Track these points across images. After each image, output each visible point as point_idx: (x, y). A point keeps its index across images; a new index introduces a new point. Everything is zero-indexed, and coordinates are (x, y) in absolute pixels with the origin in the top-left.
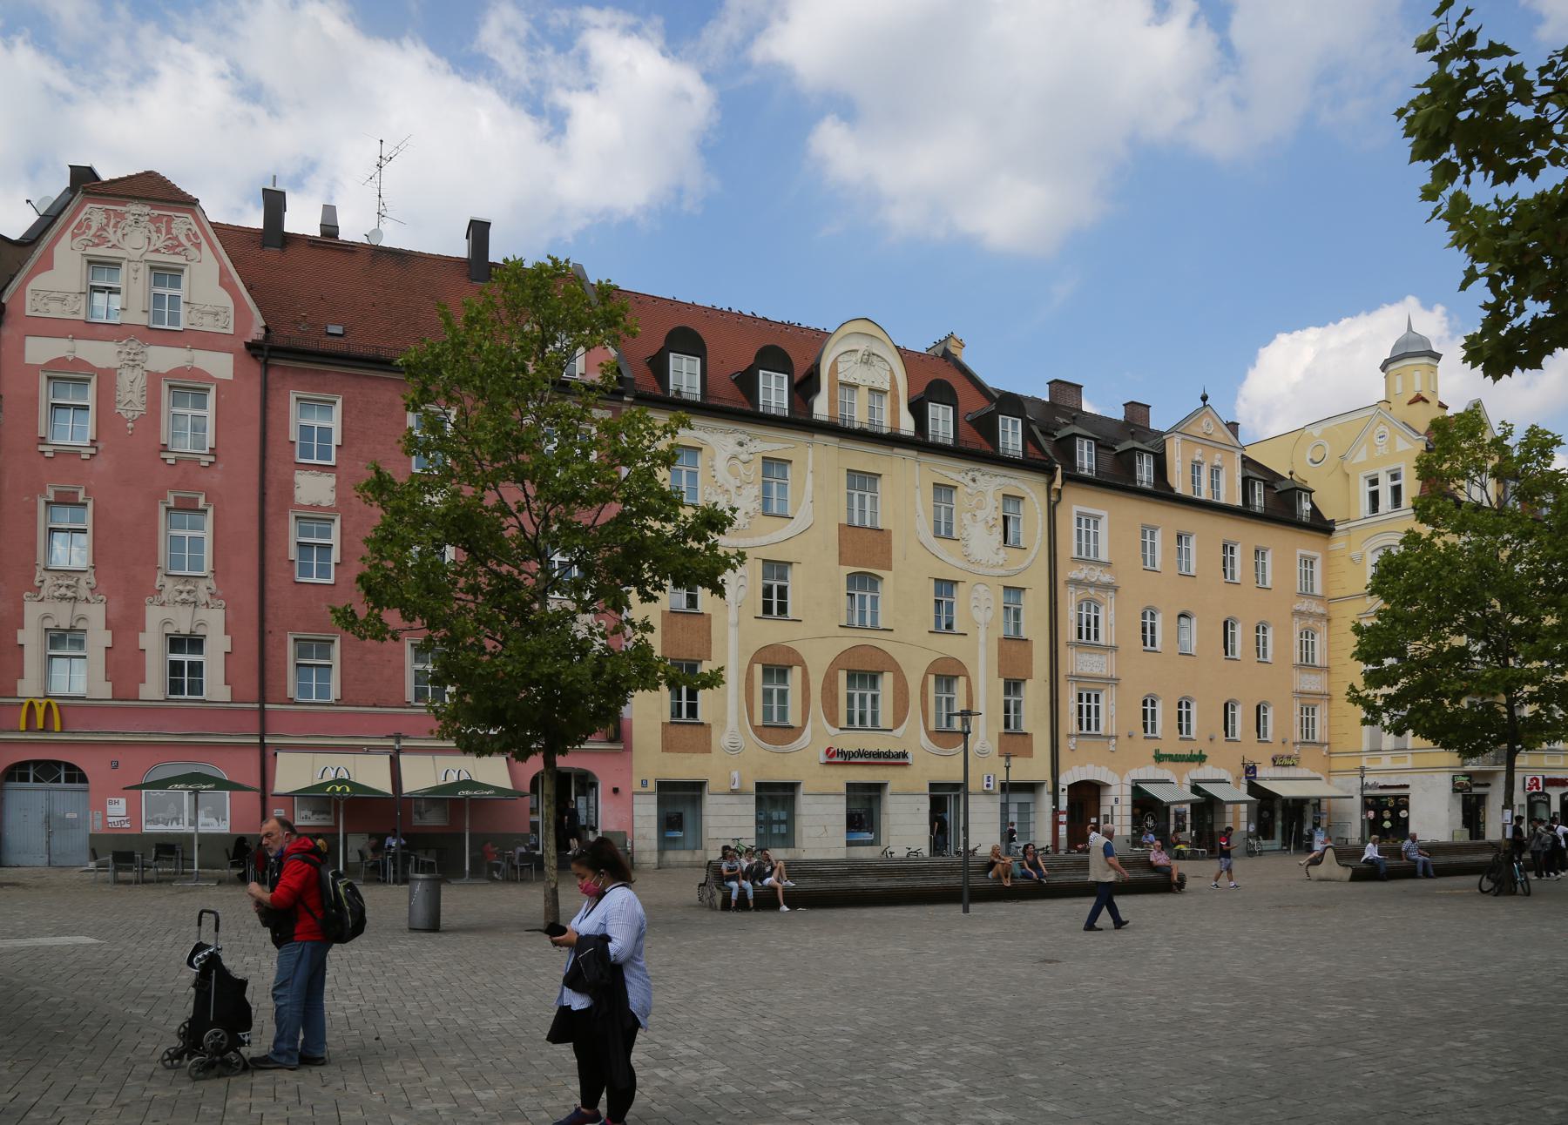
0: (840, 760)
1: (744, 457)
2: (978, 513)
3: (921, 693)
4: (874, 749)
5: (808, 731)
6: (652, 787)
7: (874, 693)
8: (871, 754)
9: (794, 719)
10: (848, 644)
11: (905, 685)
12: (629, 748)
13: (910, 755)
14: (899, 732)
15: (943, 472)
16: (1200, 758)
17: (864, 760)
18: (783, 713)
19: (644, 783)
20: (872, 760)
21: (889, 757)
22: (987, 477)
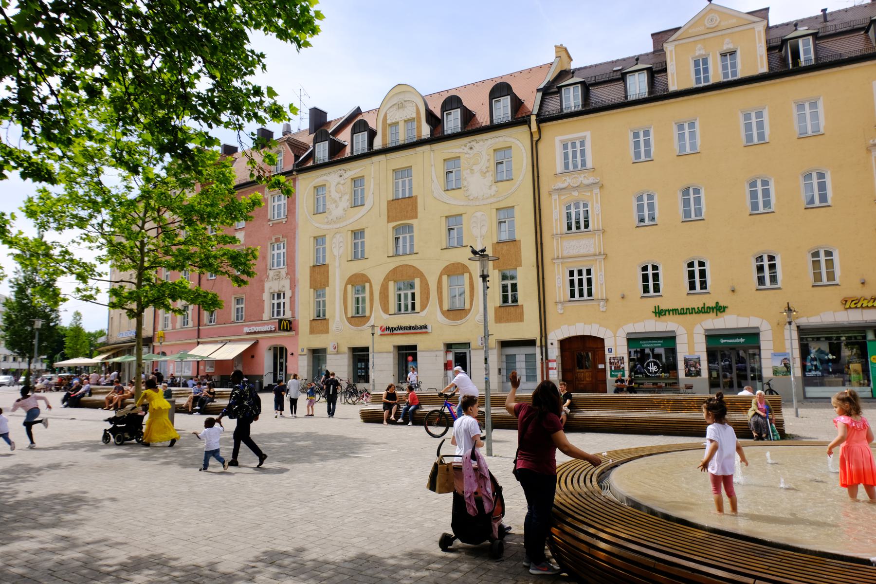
0: (388, 332)
1: (342, 182)
2: (474, 167)
3: (438, 288)
4: (407, 325)
5: (372, 318)
6: (306, 351)
7: (413, 291)
8: (406, 328)
9: (367, 314)
10: (392, 266)
11: (427, 284)
12: (297, 334)
13: (429, 327)
14: (423, 314)
15: (450, 151)
16: (719, 309)
17: (401, 332)
18: (364, 311)
19: (303, 351)
20: (406, 331)
21: (415, 329)
22: (481, 143)
